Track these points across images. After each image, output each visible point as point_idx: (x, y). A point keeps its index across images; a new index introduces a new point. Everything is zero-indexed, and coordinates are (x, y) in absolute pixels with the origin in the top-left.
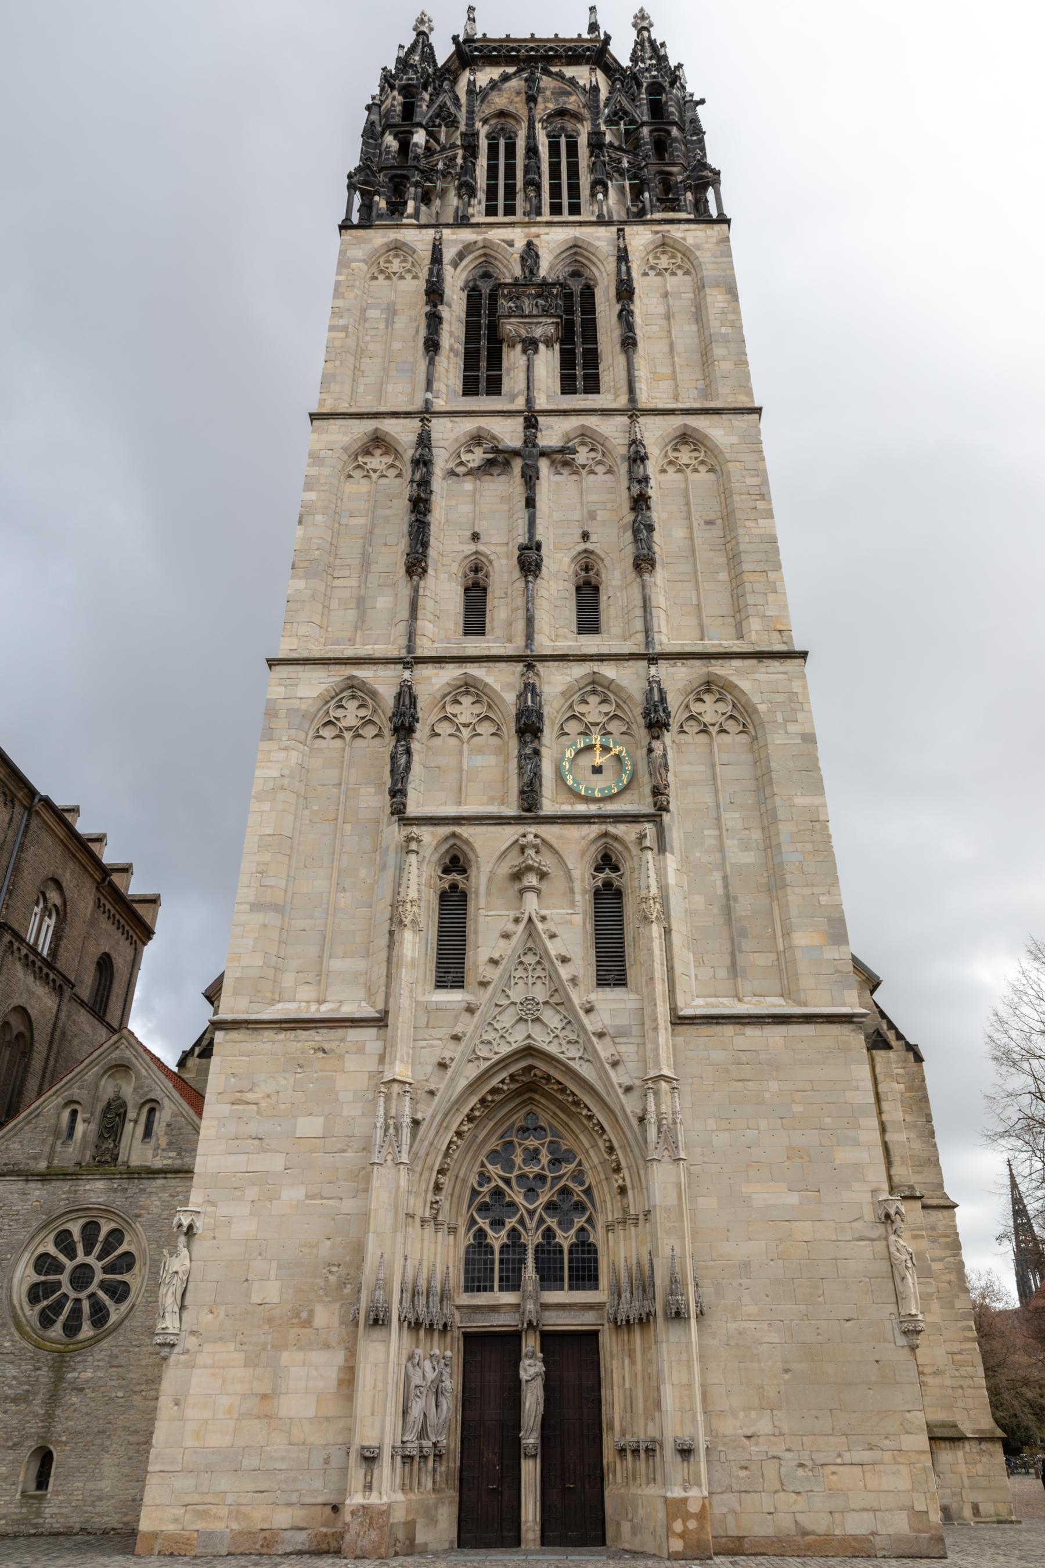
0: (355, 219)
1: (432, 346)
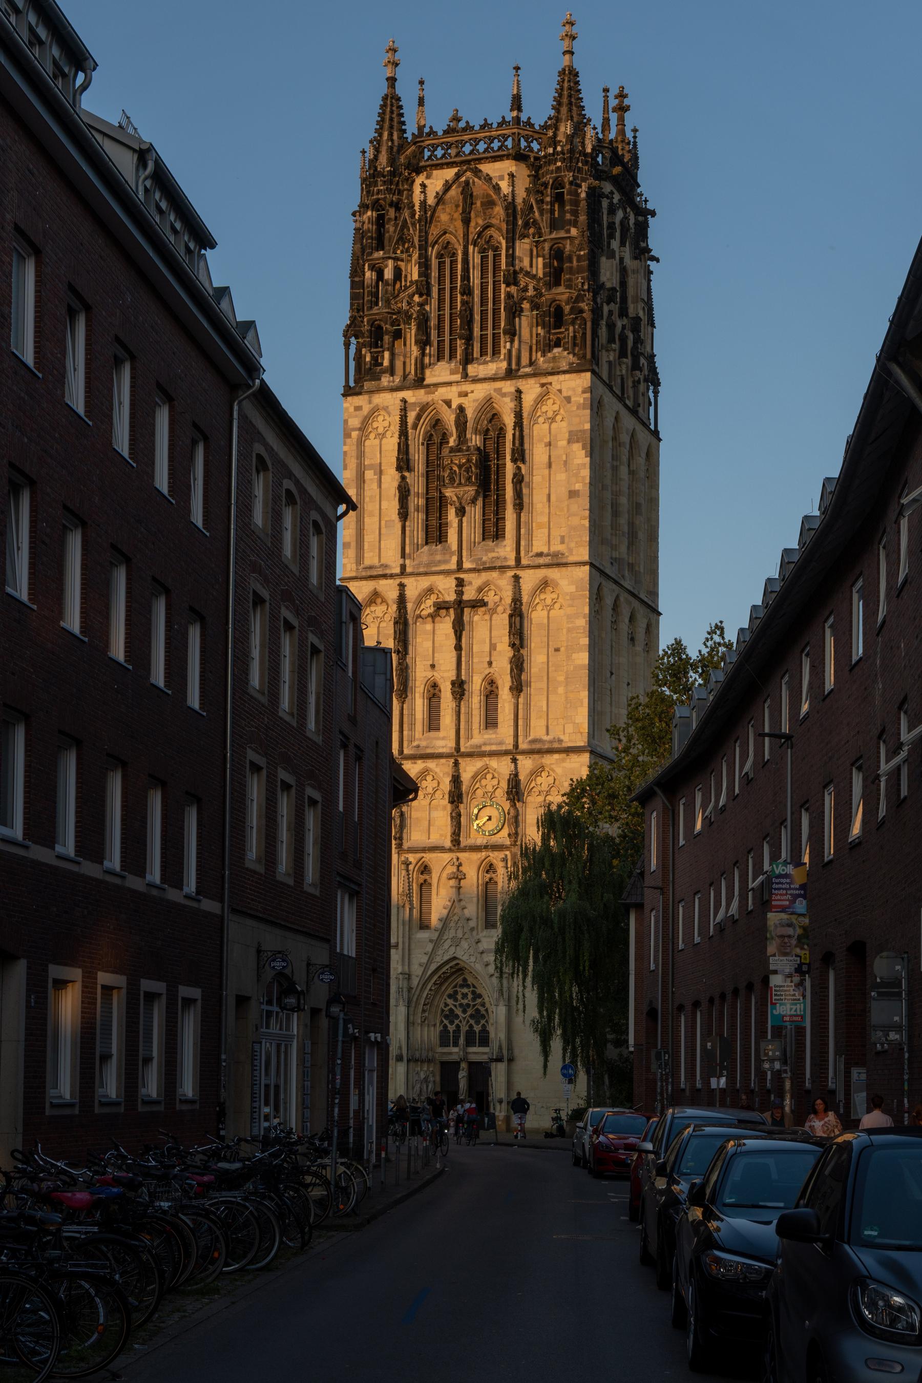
0: (352, 384)
1: (404, 515)
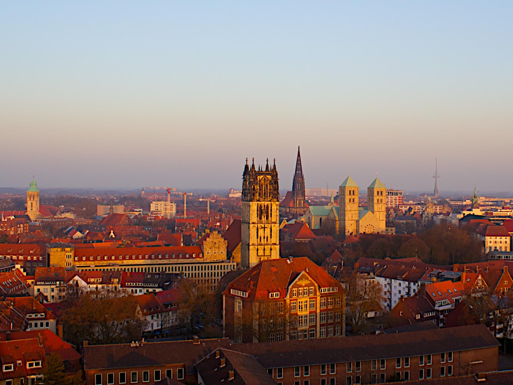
1: (258, 217)
